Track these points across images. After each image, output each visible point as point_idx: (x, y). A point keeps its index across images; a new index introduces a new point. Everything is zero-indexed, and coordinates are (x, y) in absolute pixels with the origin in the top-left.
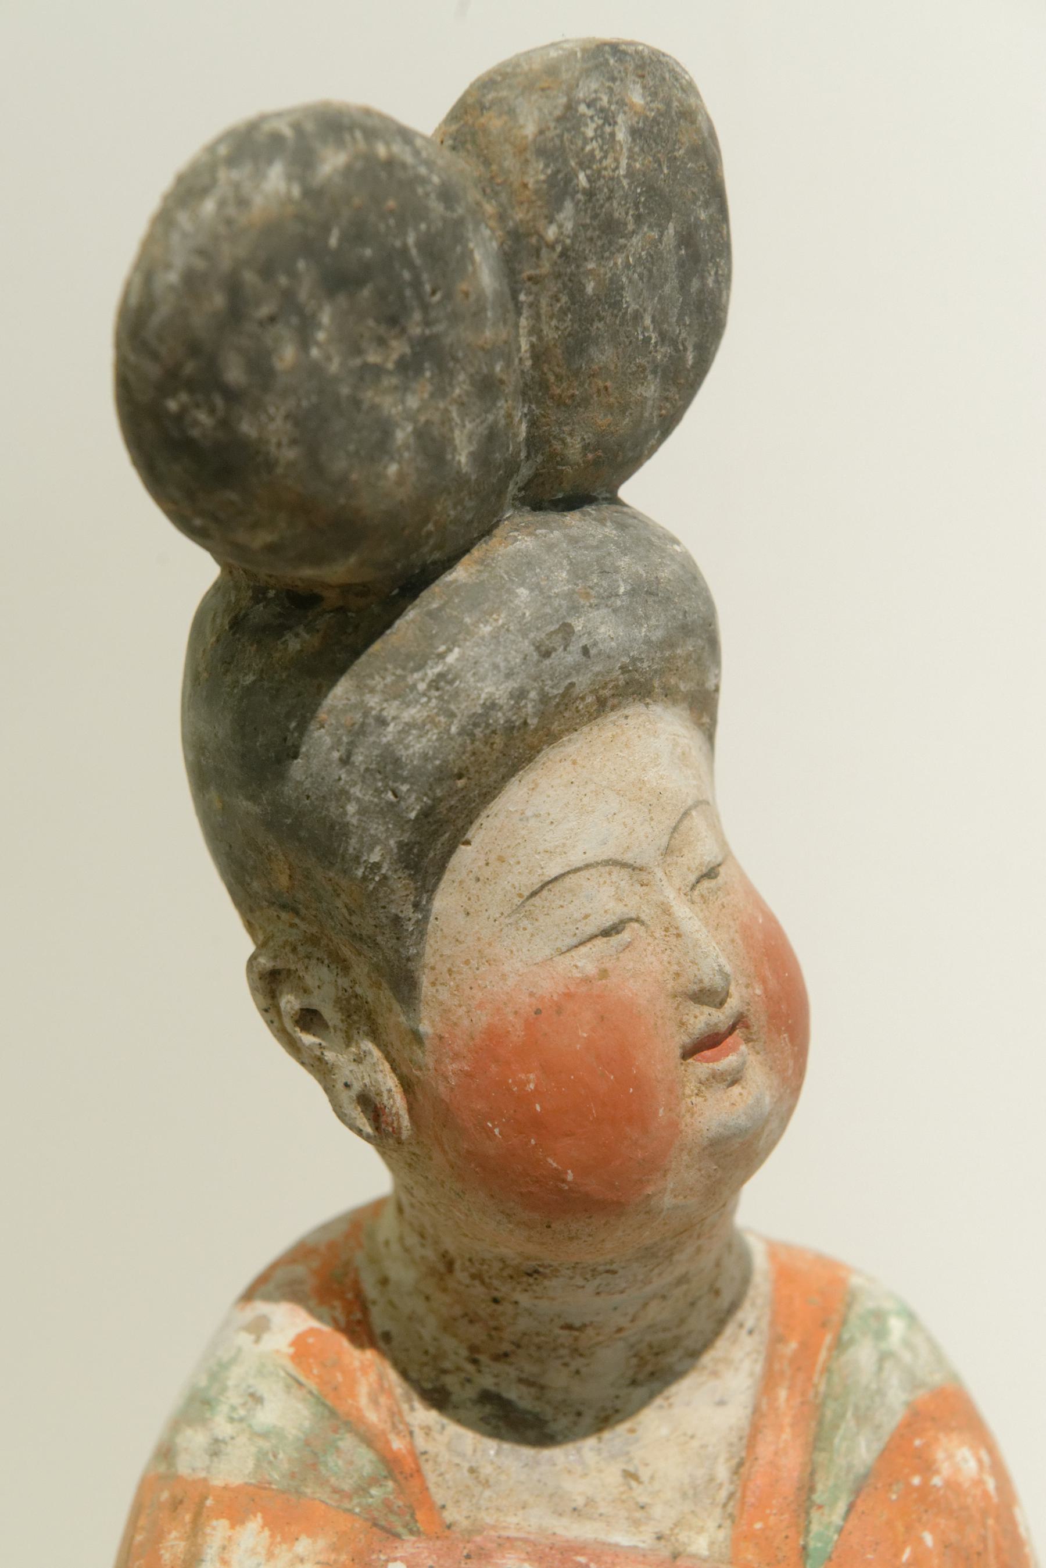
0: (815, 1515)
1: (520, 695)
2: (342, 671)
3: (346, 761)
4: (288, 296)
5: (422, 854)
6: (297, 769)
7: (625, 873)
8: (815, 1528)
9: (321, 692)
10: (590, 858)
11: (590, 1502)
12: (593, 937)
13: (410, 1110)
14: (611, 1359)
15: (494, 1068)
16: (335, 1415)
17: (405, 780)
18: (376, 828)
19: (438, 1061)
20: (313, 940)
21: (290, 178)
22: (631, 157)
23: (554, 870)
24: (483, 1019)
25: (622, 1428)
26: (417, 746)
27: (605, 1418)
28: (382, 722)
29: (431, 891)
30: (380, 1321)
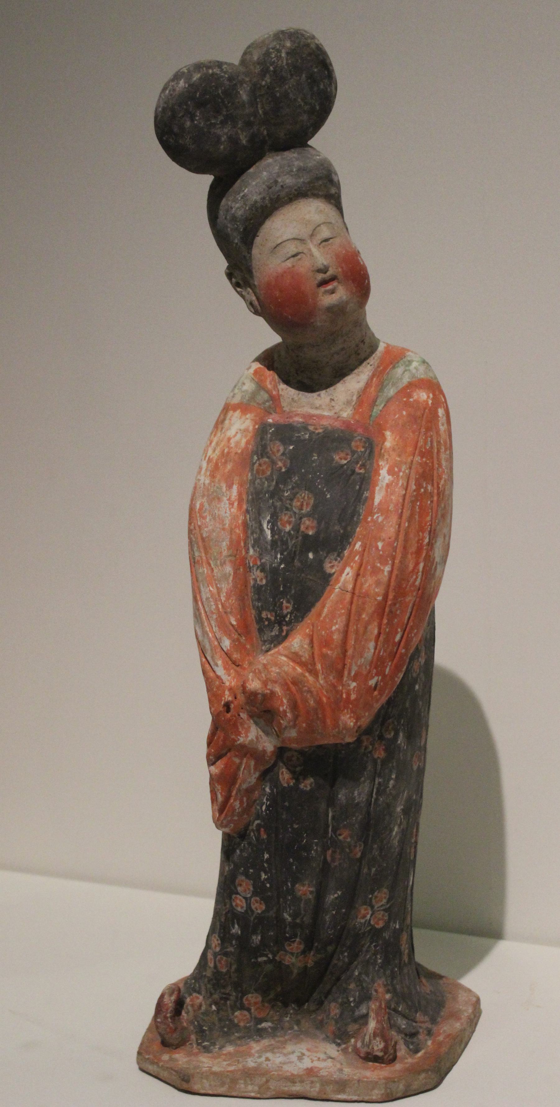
0: (375, 407)
3: (226, 218)
7: (298, 241)
10: (288, 238)
11: (320, 406)
13: (259, 304)
16: (260, 386)
18: (235, 234)
21: (185, 83)
22: (287, 60)
23: (280, 241)
25: (332, 388)
26: (240, 213)
28: (232, 208)
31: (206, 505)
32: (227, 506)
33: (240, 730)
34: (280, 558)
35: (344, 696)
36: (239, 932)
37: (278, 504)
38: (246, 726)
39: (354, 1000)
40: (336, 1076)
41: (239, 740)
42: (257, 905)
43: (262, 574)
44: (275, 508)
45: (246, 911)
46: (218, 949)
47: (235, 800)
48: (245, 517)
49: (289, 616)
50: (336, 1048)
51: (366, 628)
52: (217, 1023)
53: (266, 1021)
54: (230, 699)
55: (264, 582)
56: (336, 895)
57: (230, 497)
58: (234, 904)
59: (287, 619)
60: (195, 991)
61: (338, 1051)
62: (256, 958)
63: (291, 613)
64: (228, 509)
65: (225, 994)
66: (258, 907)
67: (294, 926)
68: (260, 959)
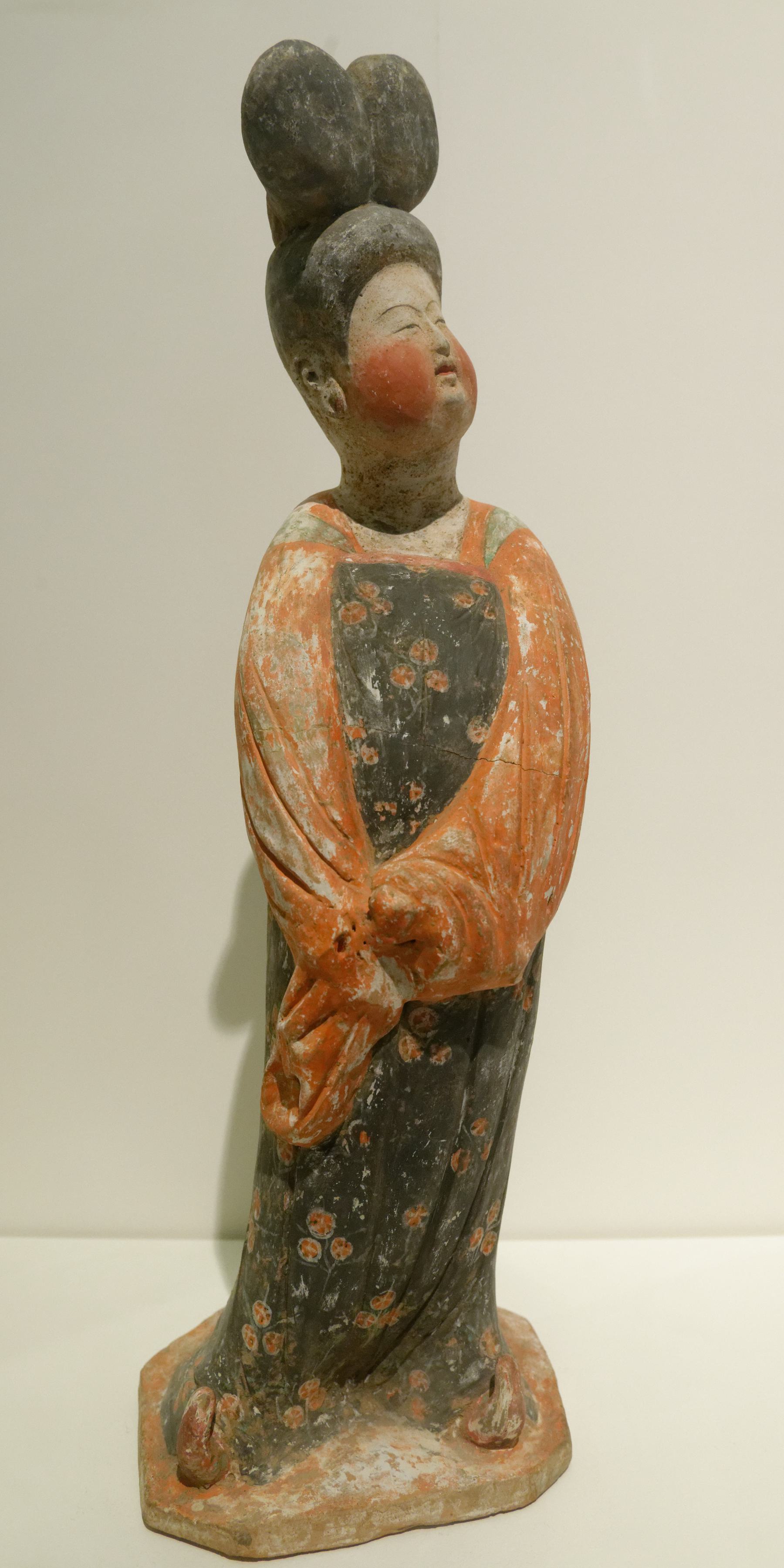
0: (487, 550)
1: (376, 242)
2: (318, 237)
3: (320, 264)
4: (297, 85)
5: (347, 296)
6: (305, 274)
7: (414, 311)
8: (487, 553)
9: (311, 245)
10: (402, 303)
12: (403, 328)
13: (346, 399)
14: (417, 507)
15: (373, 371)
16: (326, 523)
17: (340, 268)
18: (331, 287)
19: (355, 374)
20: (312, 347)
23: (390, 305)
24: (369, 355)
25: (421, 531)
26: (344, 255)
27: (416, 527)
28: (332, 248)
29: (351, 312)
30: (339, 503)
31: (275, 659)
32: (308, 660)
33: (359, 978)
34: (401, 725)
35: (520, 913)
36: (307, 1294)
37: (387, 655)
38: (367, 971)
39: (456, 1364)
40: (462, 1484)
41: (355, 993)
42: (340, 1249)
43: (372, 749)
44: (383, 660)
45: (321, 1261)
46: (266, 1323)
47: (333, 1091)
48: (335, 675)
49: (419, 806)
50: (434, 1436)
51: (545, 813)
52: (262, 1433)
53: (322, 1413)
54: (347, 929)
55: (376, 760)
56: (454, 1218)
57: (310, 649)
58: (301, 1253)
59: (417, 811)
60: (226, 1390)
61: (438, 1440)
62: (327, 1329)
63: (423, 802)
64: (309, 664)
65: (272, 1387)
66: (341, 1251)
67: (391, 1270)
68: (331, 1329)
